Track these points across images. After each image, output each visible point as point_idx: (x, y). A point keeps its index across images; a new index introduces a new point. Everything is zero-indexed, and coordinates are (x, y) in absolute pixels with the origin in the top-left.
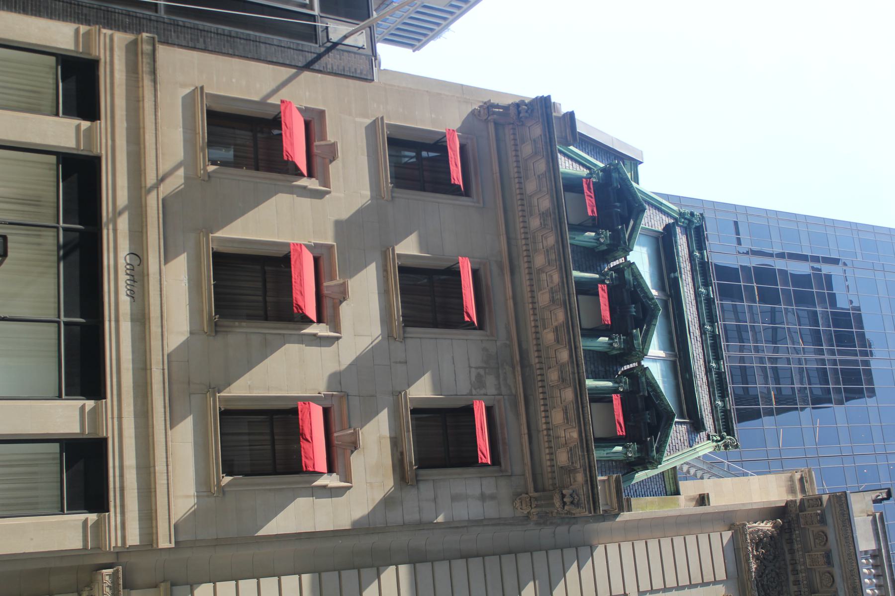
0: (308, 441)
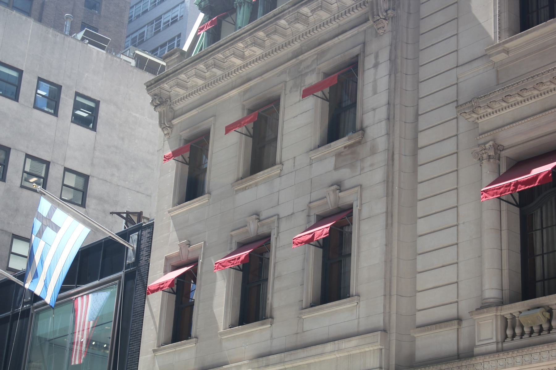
0: (314, 235)
